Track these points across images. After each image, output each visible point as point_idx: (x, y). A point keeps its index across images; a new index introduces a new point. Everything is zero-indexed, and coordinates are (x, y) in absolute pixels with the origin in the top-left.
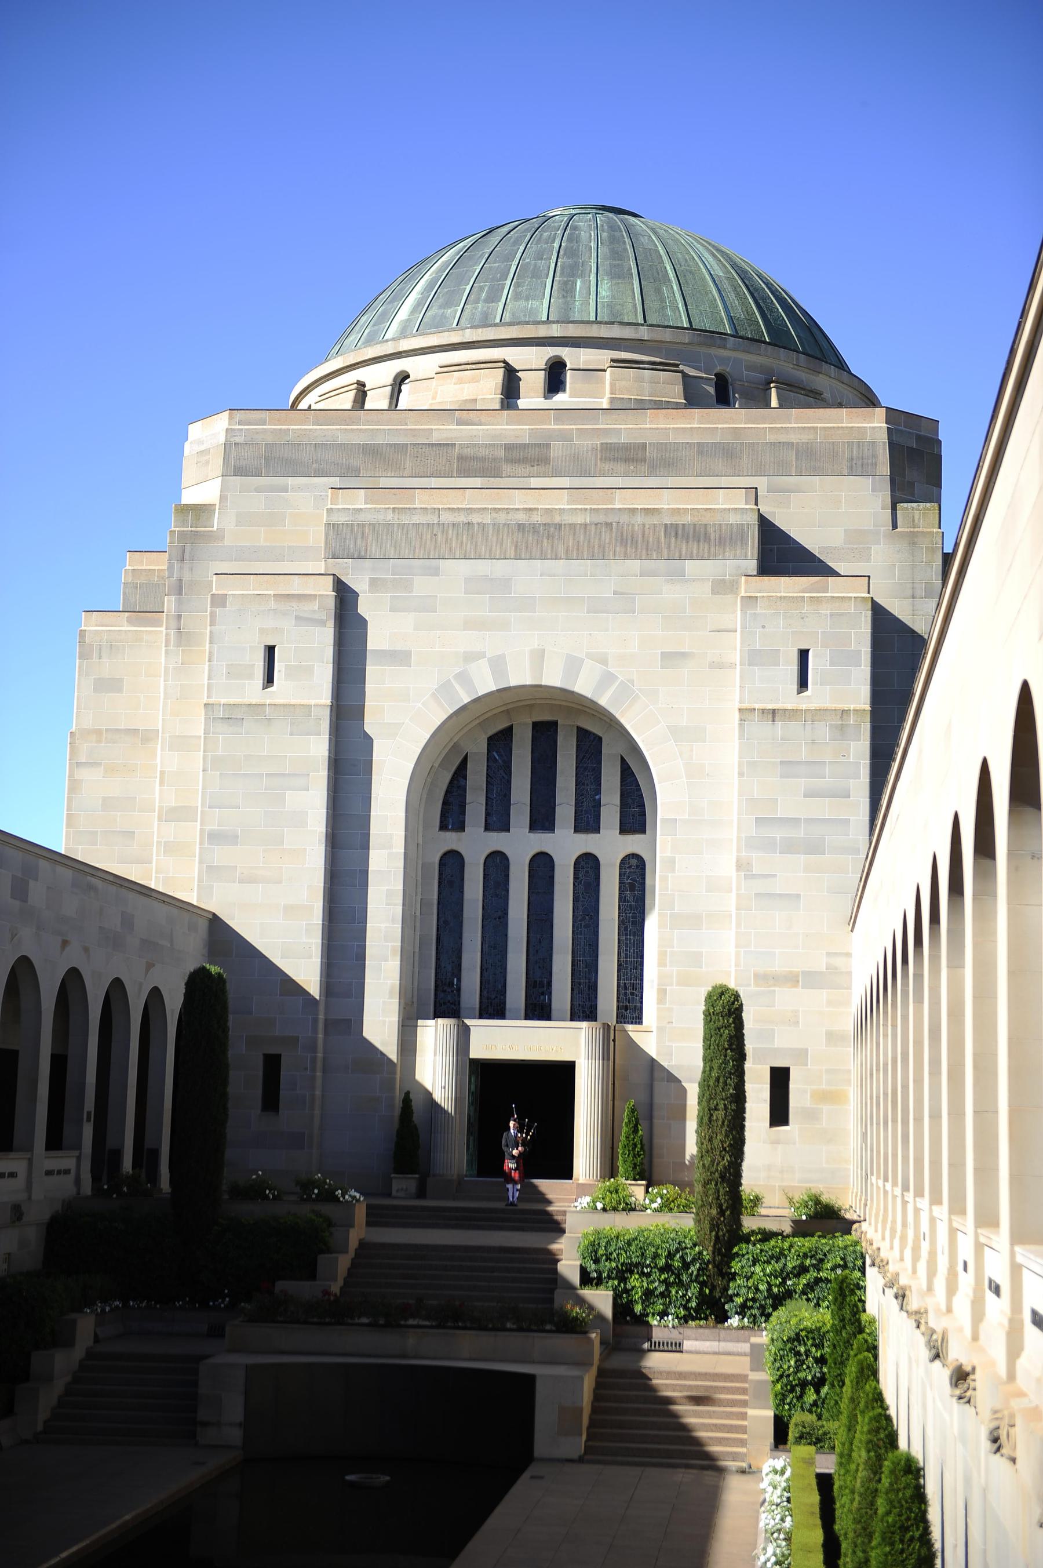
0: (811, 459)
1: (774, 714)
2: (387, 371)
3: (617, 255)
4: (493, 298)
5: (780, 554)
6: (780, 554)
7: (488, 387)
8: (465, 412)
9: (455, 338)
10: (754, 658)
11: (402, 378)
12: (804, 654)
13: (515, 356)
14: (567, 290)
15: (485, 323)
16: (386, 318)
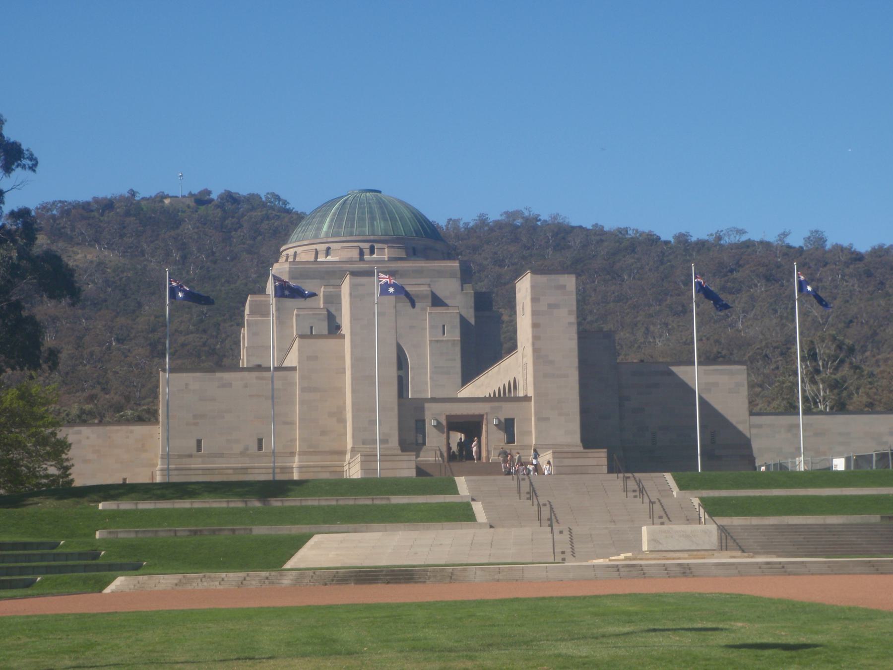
0: (441, 274)
1: (437, 341)
2: (323, 247)
3: (383, 213)
4: (352, 226)
5: (437, 301)
6: (437, 301)
7: (355, 254)
8: (350, 261)
9: (344, 239)
10: (431, 327)
11: (329, 249)
12: (444, 326)
13: (362, 245)
14: (372, 225)
15: (351, 235)
16: (319, 229)
